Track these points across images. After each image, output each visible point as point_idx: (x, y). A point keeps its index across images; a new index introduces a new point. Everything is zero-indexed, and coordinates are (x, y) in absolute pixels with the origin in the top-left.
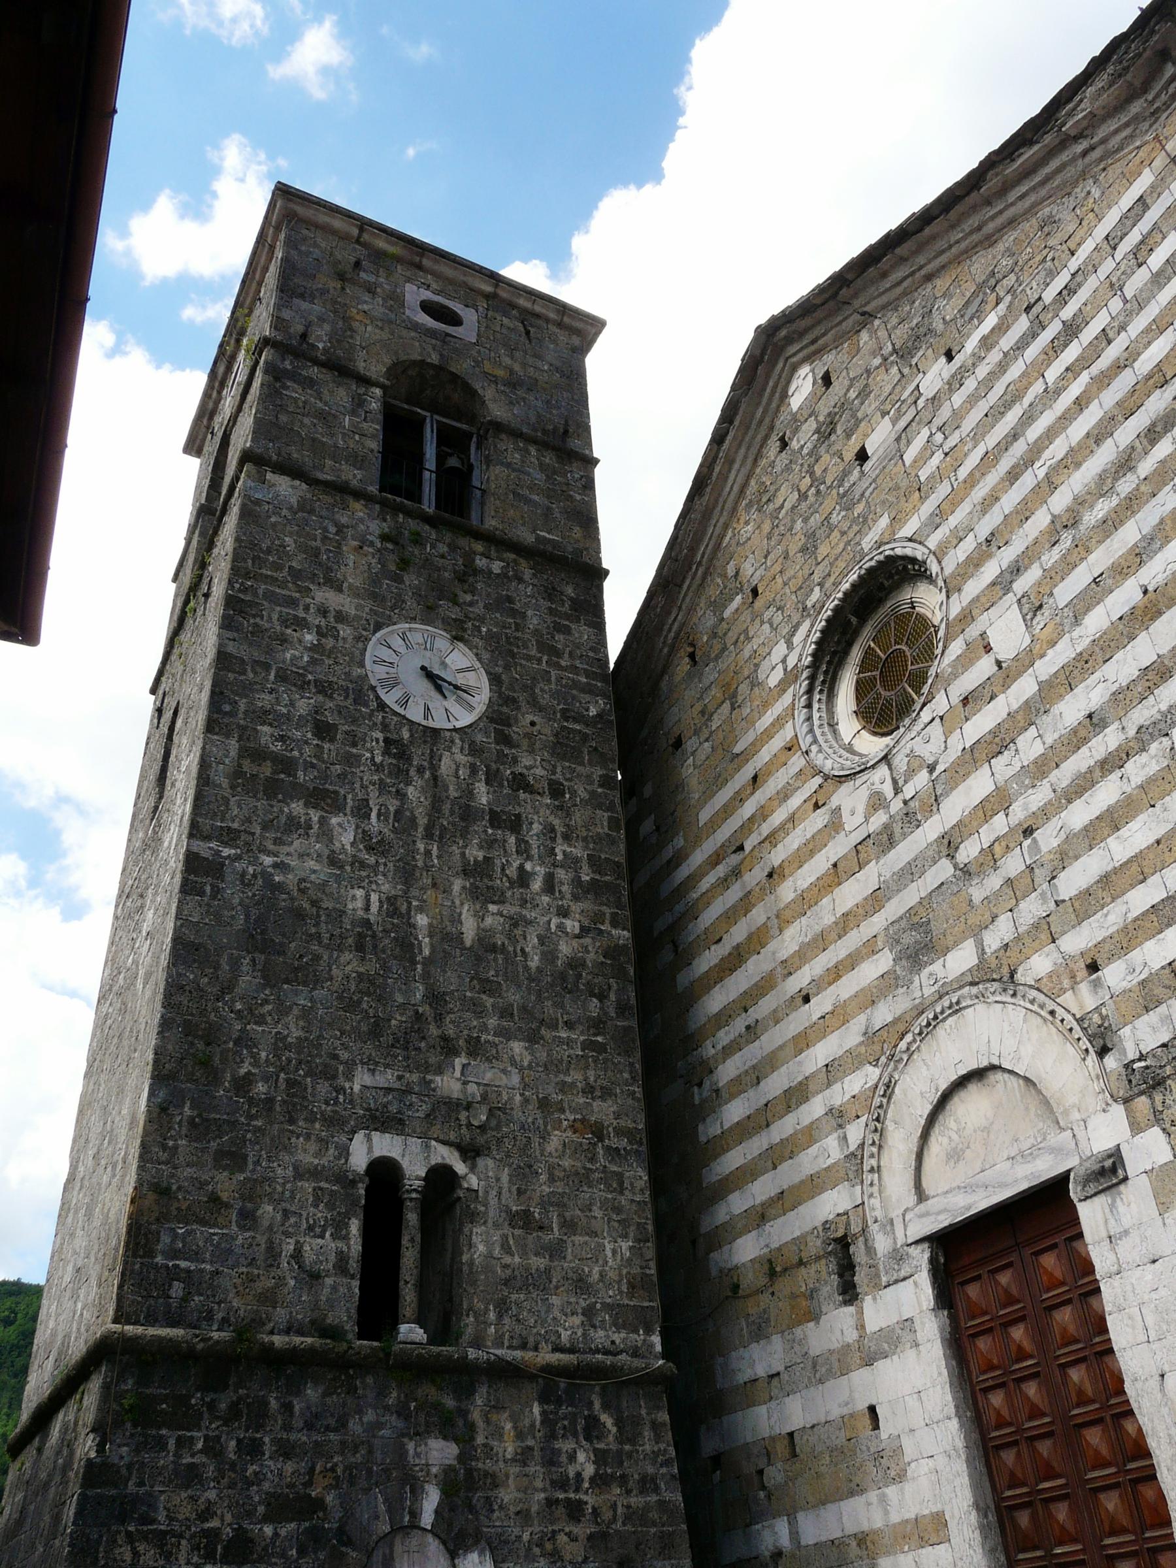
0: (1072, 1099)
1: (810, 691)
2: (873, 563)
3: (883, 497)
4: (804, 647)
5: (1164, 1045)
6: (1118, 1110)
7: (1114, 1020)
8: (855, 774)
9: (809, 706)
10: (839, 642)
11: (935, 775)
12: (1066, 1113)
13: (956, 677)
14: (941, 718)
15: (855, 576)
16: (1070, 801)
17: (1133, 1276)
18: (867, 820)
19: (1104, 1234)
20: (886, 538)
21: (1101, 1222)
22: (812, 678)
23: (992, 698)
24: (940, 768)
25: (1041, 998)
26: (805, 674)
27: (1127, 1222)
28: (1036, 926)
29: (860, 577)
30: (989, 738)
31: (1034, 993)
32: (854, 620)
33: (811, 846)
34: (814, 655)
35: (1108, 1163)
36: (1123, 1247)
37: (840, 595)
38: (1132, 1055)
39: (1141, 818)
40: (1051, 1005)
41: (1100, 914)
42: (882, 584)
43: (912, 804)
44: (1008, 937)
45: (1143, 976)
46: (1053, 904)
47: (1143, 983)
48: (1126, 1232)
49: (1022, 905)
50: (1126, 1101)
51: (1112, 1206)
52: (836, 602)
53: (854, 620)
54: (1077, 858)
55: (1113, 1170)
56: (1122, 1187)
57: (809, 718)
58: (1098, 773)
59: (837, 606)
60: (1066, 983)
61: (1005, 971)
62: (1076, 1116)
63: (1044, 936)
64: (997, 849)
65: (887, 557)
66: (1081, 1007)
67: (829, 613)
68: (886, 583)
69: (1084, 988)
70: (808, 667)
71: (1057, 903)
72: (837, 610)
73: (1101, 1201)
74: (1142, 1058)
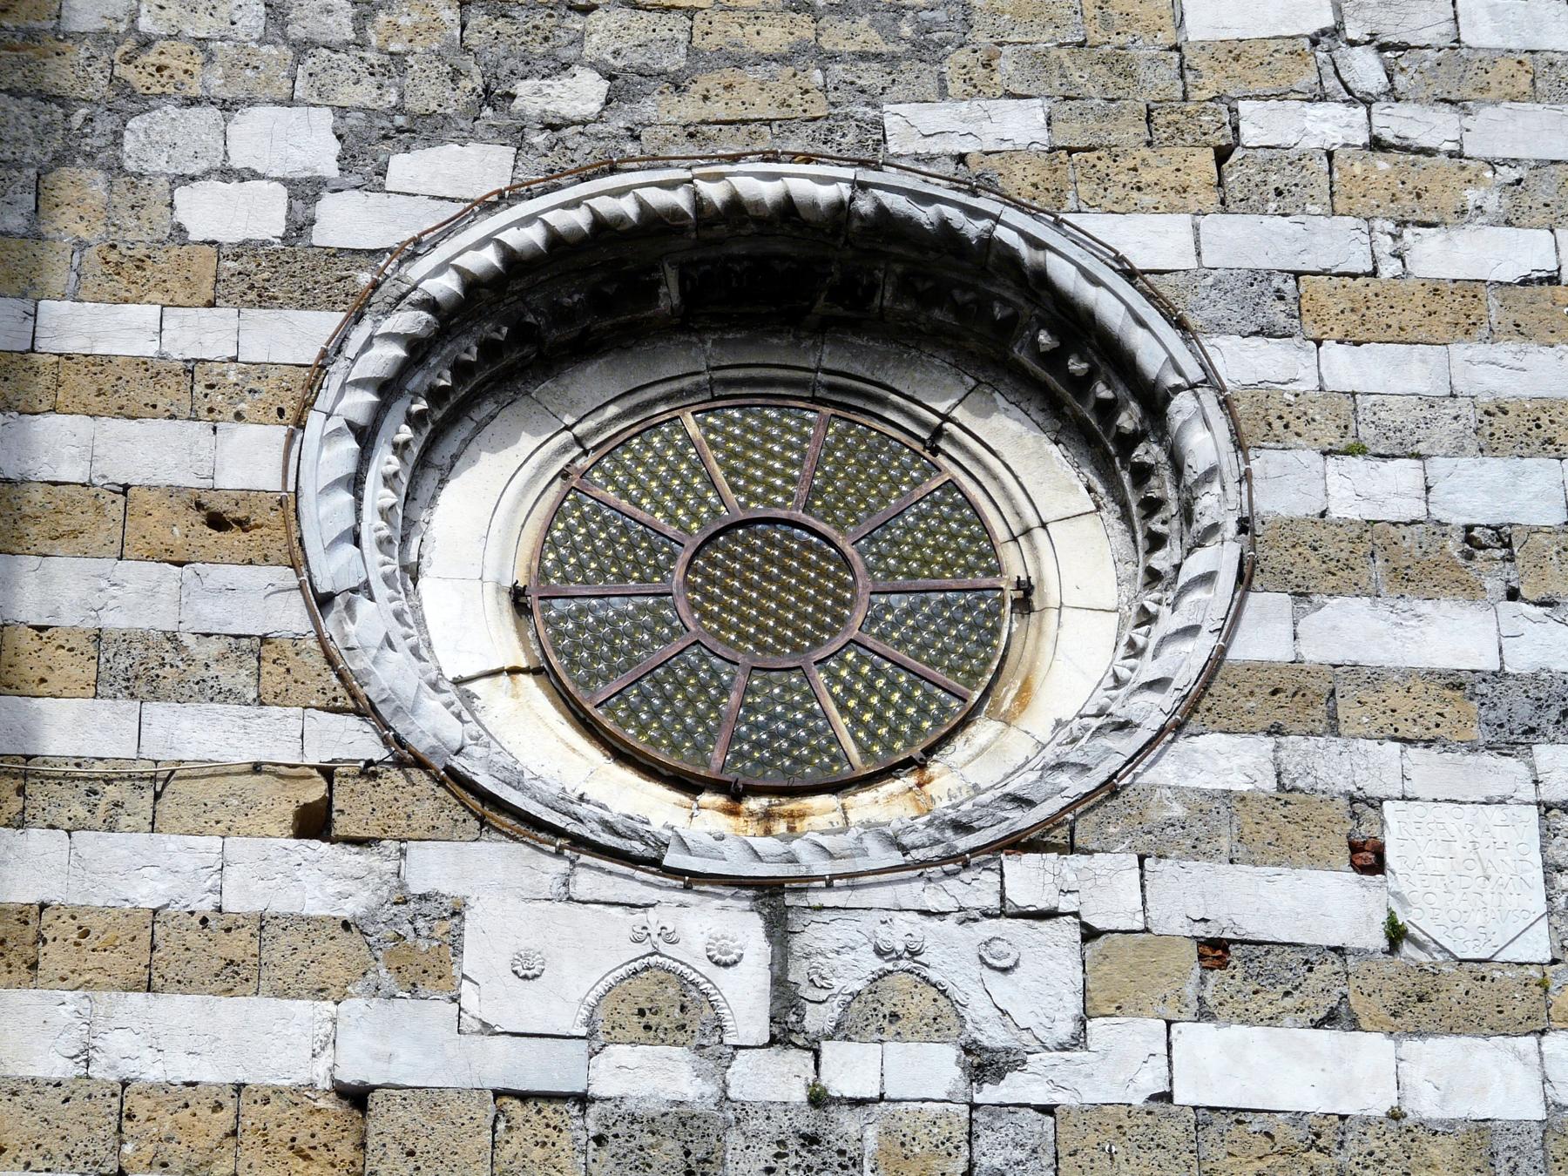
1: (388, 389)
2: (926, 215)
3: (1044, 40)
4: (449, 228)
8: (579, 843)
9: (365, 436)
10: (562, 316)
11: (989, 1094)
13: (1196, 851)
14: (1090, 934)
15: (826, 194)
18: (594, 1038)
20: (1018, 181)
22: (418, 350)
23: (1329, 1020)
24: (1011, 1088)
26: (410, 321)
29: (841, 209)
30: (1288, 1134)
32: (670, 295)
33: (239, 946)
34: (472, 284)
37: (715, 193)
42: (873, 288)
43: (848, 1123)
52: (680, 199)
53: (670, 295)
57: (355, 483)
59: (675, 213)
65: (988, 242)
67: (627, 207)
68: (886, 297)
70: (430, 305)
72: (656, 224)
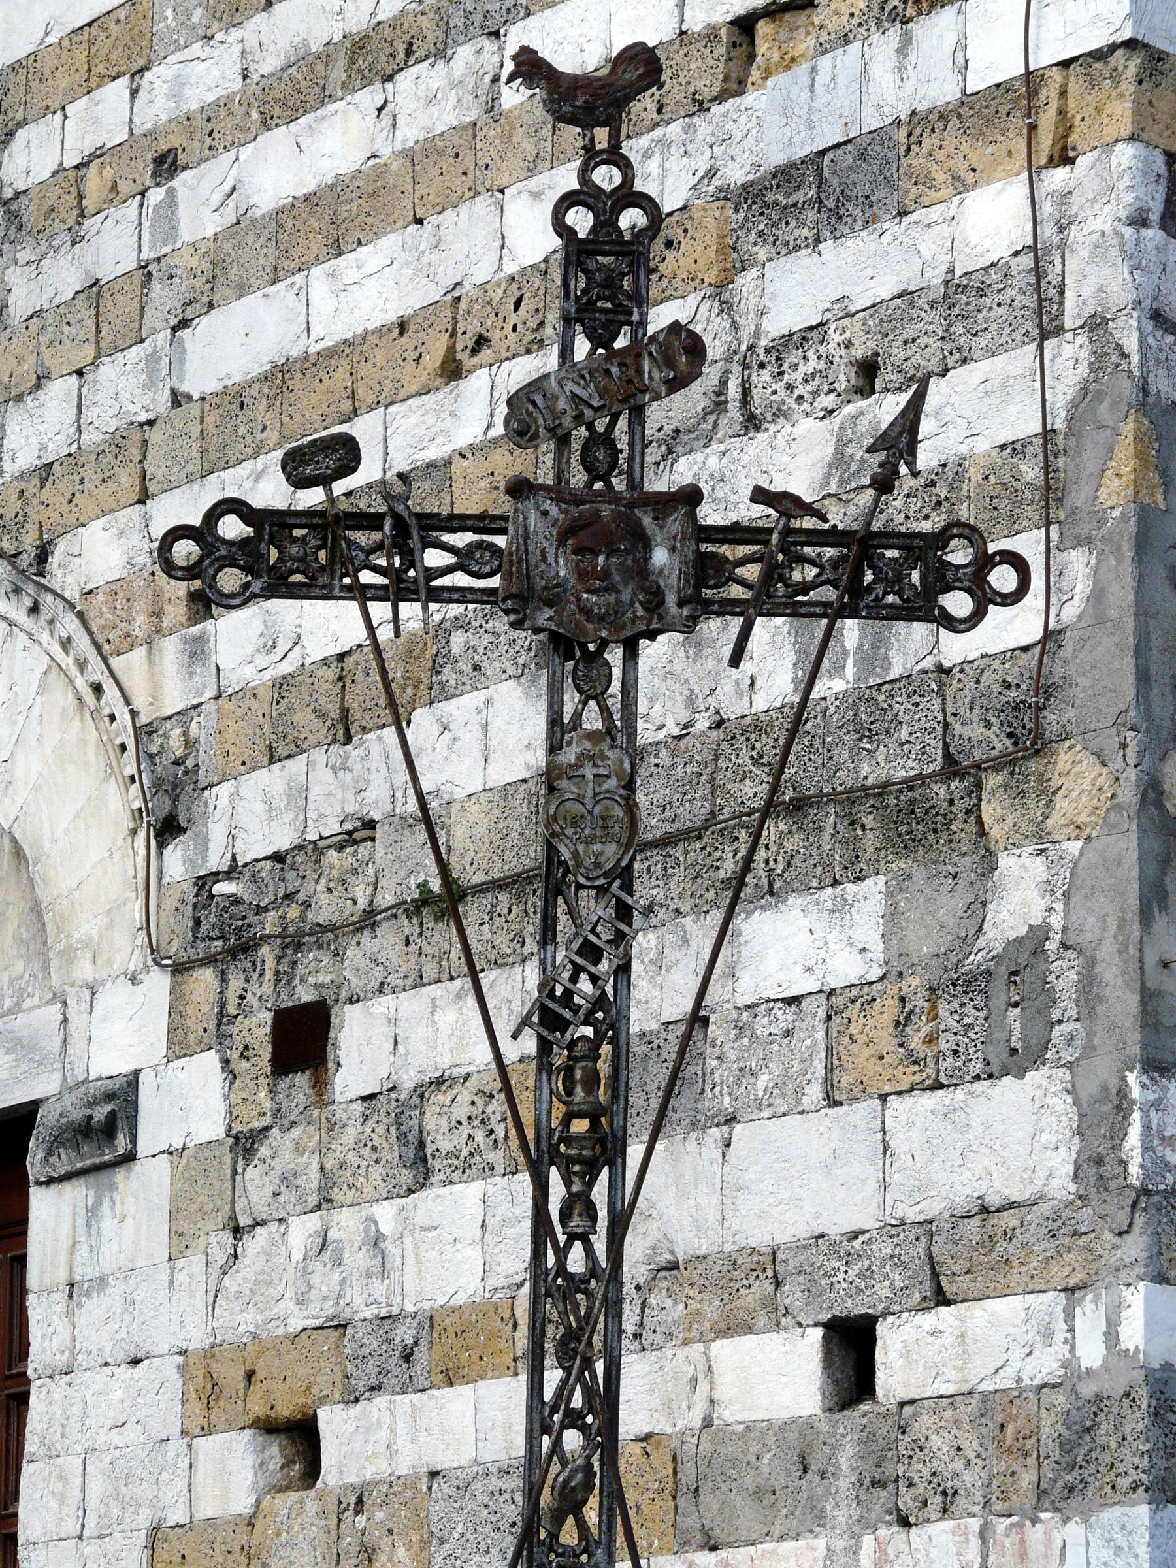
0: (87, 926)
5: (278, 857)
6: (159, 983)
7: (207, 758)
12: (69, 955)
16: (267, 122)
17: (93, 1382)
19: (62, 1276)
21: (65, 1244)
25: (82, 642)
27: (111, 1257)
28: (117, 443)
31: (70, 625)
35: (100, 1113)
36: (93, 1309)
38: (216, 861)
39: (389, 243)
40: (96, 671)
41: (248, 466)
44: (57, 448)
45: (286, 668)
46: (165, 397)
47: (282, 684)
48: (102, 1282)
49: (107, 371)
50: (179, 969)
51: (93, 1213)
54: (243, 290)
55: (109, 1130)
56: (120, 1174)
58: (338, 73)
60: (140, 624)
61: (29, 540)
62: (85, 970)
63: (127, 479)
64: (94, 184)
66: (155, 697)
69: (171, 648)
71: (177, 399)
73: (76, 1193)
74: (232, 872)
